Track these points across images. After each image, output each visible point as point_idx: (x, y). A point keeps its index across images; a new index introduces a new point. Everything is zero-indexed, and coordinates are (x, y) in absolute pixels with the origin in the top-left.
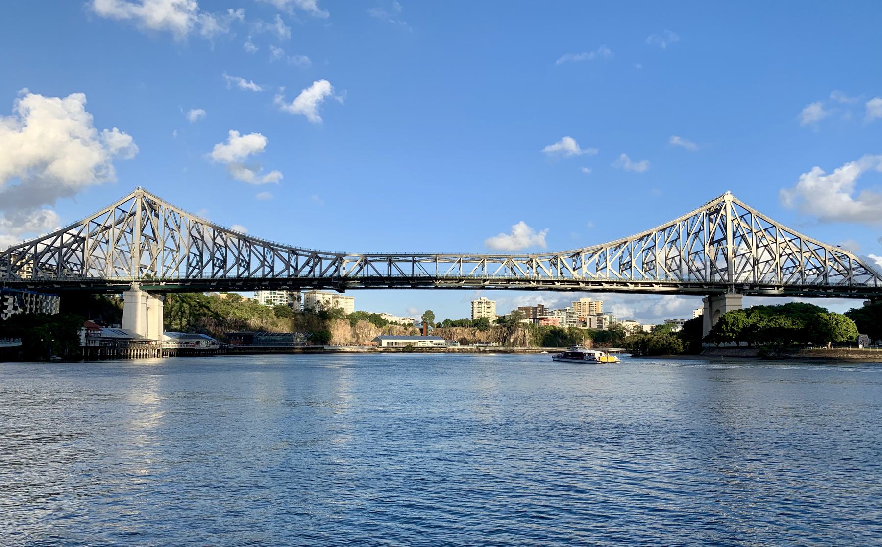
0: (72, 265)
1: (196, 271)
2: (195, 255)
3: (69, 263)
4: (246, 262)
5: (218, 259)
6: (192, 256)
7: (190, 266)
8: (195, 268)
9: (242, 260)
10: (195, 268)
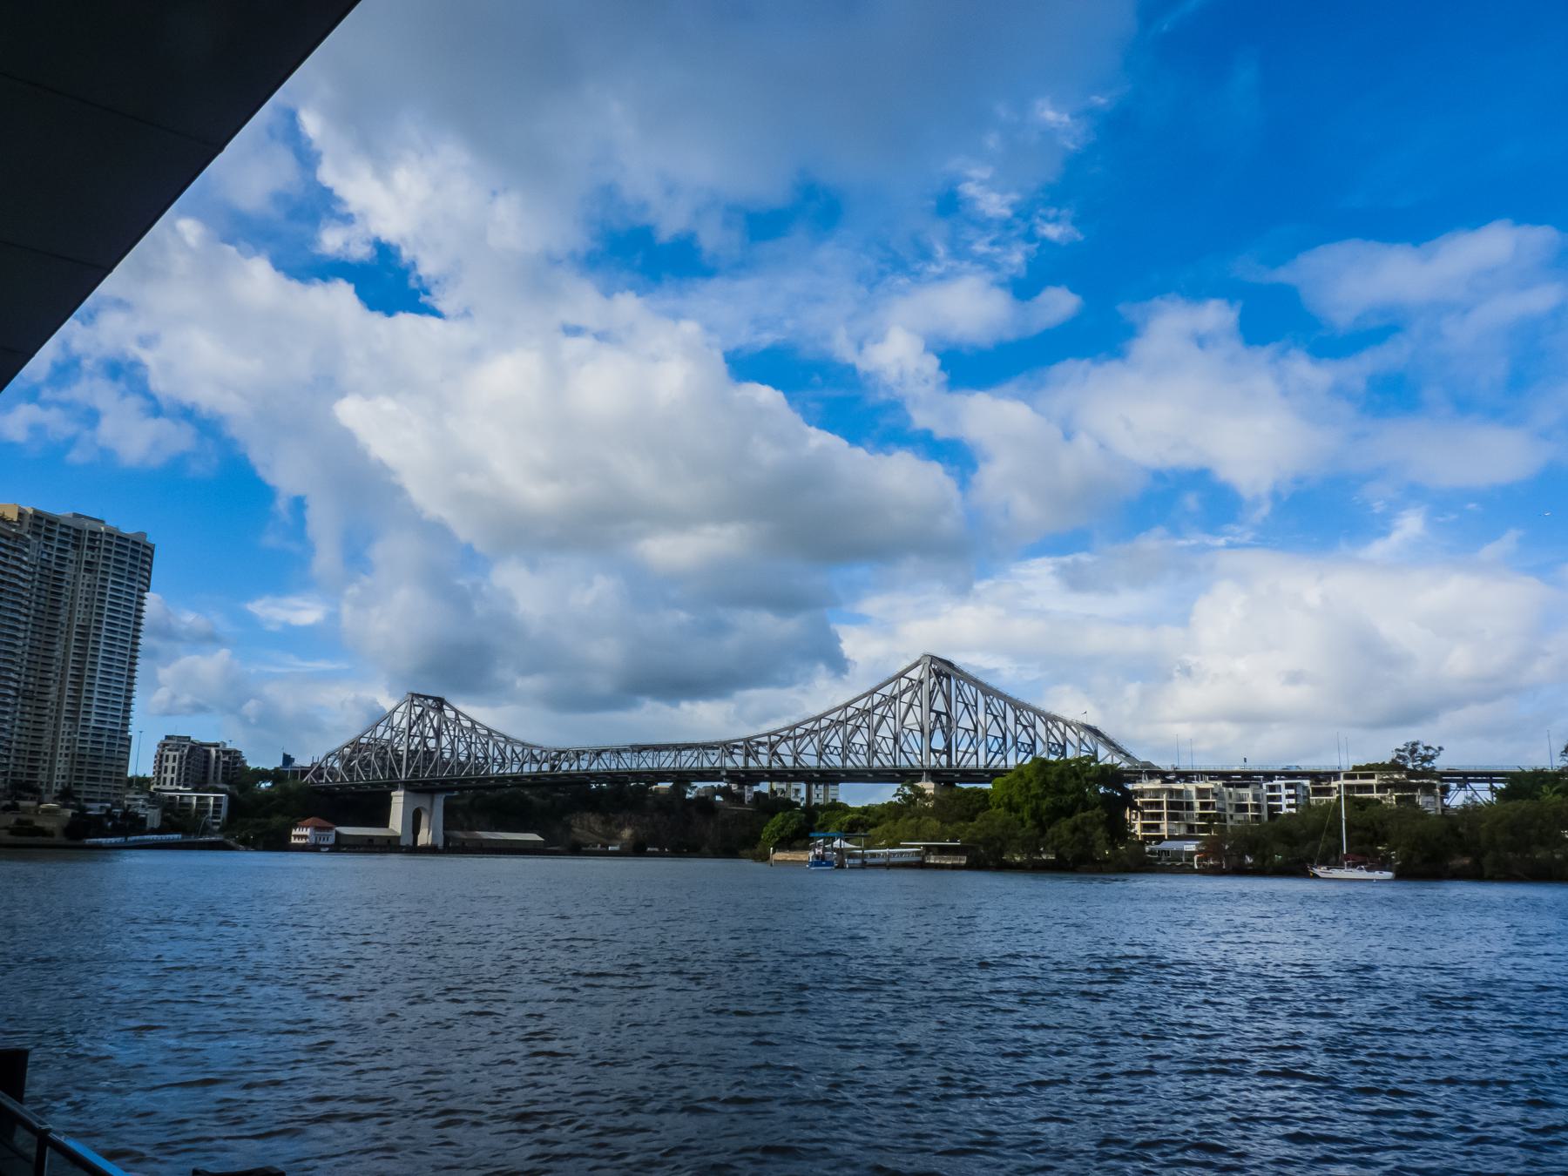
0: (832, 749)
1: (999, 757)
2: (996, 738)
3: (854, 744)
4: (1059, 745)
5: (1023, 744)
6: (990, 740)
7: (990, 751)
8: (996, 753)
9: (1053, 744)
10: (996, 753)
